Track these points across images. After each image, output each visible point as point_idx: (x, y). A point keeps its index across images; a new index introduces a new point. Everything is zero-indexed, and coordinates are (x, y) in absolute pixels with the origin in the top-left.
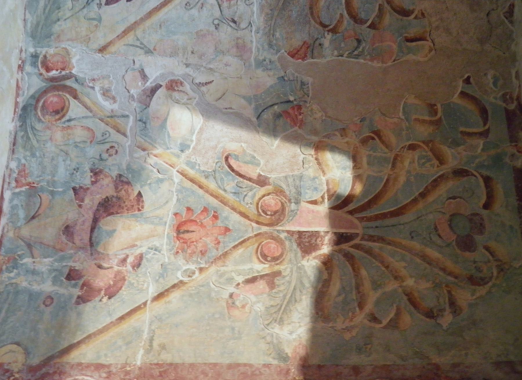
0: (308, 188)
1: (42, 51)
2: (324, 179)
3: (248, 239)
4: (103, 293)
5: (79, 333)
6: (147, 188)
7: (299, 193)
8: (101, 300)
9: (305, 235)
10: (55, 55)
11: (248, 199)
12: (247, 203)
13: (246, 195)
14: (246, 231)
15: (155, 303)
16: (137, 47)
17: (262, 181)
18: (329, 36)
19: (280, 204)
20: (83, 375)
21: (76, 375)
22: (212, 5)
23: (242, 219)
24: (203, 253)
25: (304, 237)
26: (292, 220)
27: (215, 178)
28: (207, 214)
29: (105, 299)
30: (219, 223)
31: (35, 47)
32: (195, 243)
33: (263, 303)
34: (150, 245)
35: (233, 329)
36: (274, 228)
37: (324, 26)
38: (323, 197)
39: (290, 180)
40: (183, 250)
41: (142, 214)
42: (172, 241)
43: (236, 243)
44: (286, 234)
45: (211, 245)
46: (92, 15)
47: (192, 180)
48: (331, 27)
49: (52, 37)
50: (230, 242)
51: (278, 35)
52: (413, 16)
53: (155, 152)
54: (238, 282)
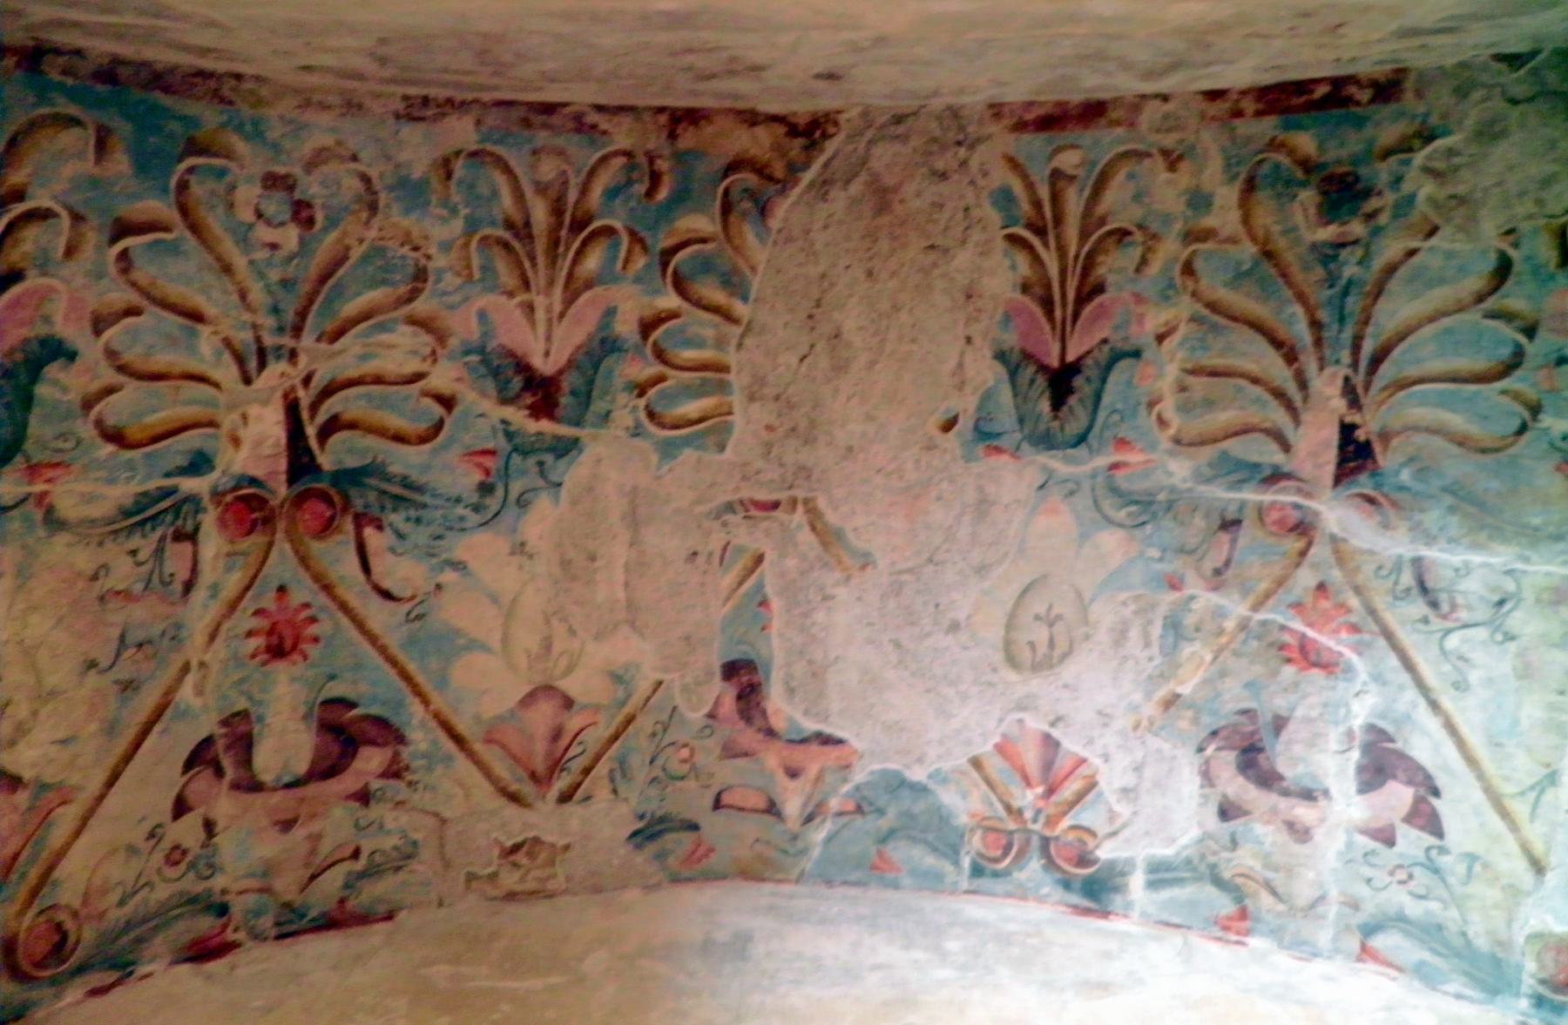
1: (1528, 983)
10: (1542, 967)
16: (1538, 799)
18: (1546, 420)
22: (1464, 641)
31: (1517, 995)
37: (1523, 429)
46: (1461, 869)
48: (1526, 415)
49: (1500, 955)
51: (1536, 521)
52: (1512, 253)
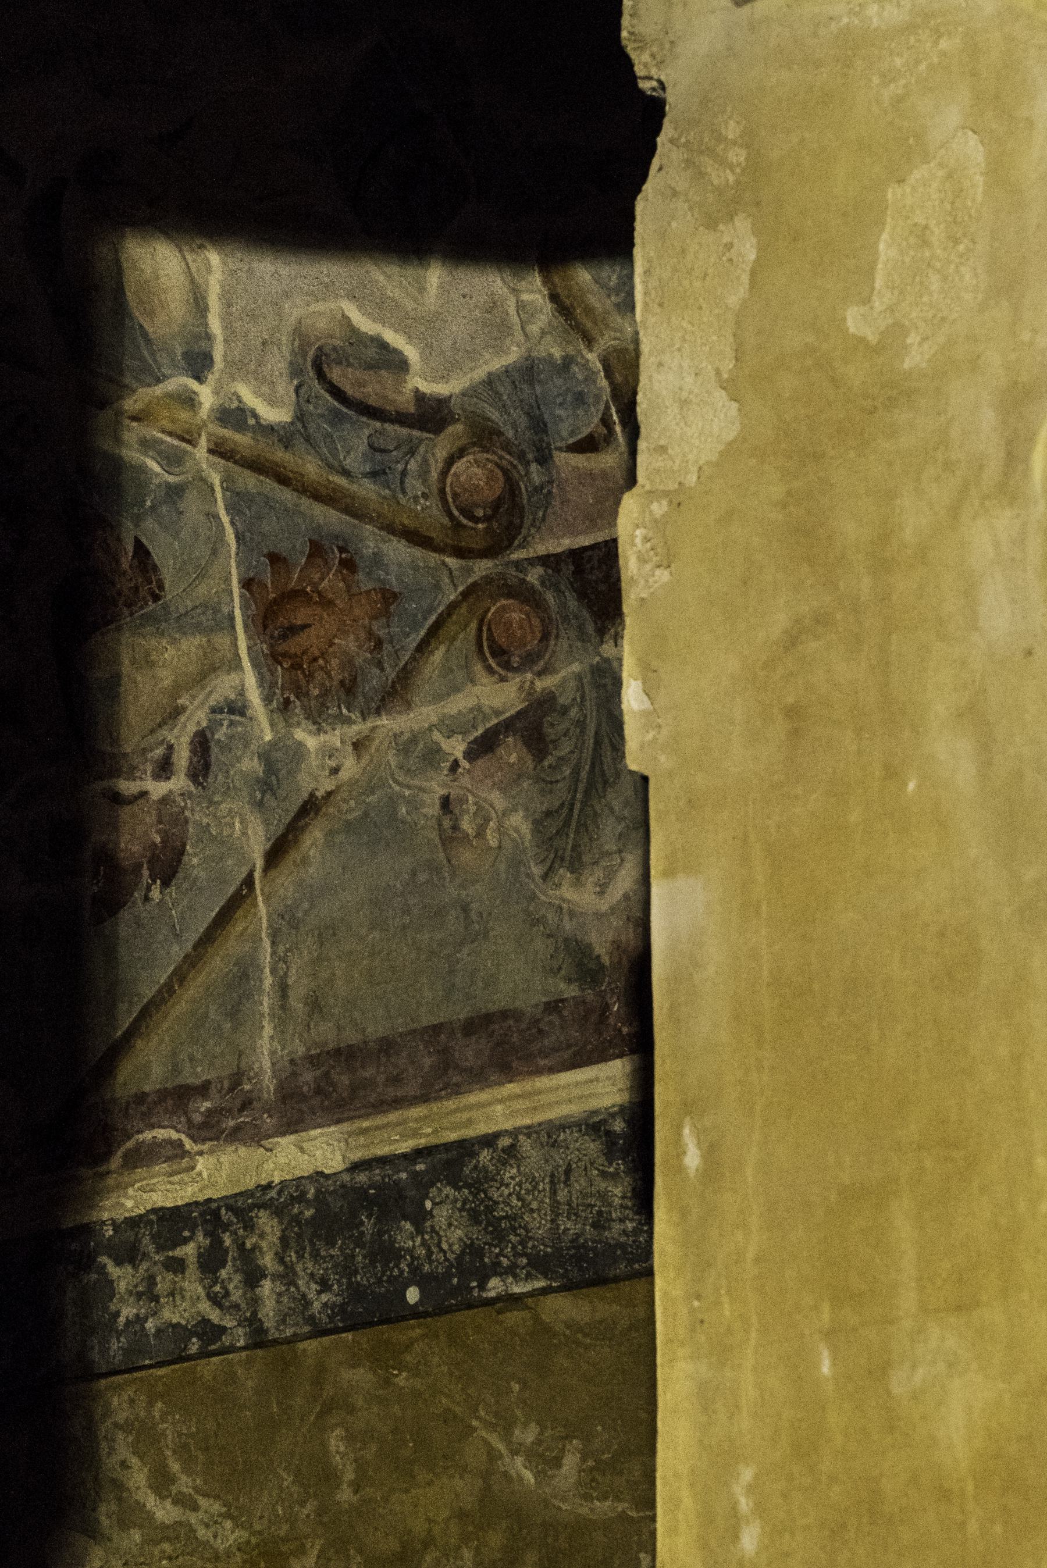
0: (559, 400)
2: (593, 358)
3: (452, 607)
4: (146, 873)
5: (123, 1007)
6: (149, 523)
7: (539, 426)
8: (147, 899)
9: (590, 558)
11: (415, 485)
12: (416, 498)
13: (404, 473)
14: (437, 586)
15: (273, 873)
17: (431, 415)
19: (499, 473)
20: (152, 1127)
21: (140, 1132)
23: (418, 552)
24: (349, 688)
25: (588, 566)
26: (543, 520)
27: (308, 439)
28: (326, 563)
29: (155, 894)
30: (365, 583)
32: (321, 662)
33: (527, 809)
34: (212, 702)
35: (465, 909)
36: (506, 559)
38: (606, 421)
39: (505, 390)
40: (301, 693)
41: (165, 607)
42: (265, 670)
43: (422, 633)
44: (539, 570)
45: (361, 658)
47: (256, 465)
50: (408, 635)
53: (130, 405)
54: (452, 759)
